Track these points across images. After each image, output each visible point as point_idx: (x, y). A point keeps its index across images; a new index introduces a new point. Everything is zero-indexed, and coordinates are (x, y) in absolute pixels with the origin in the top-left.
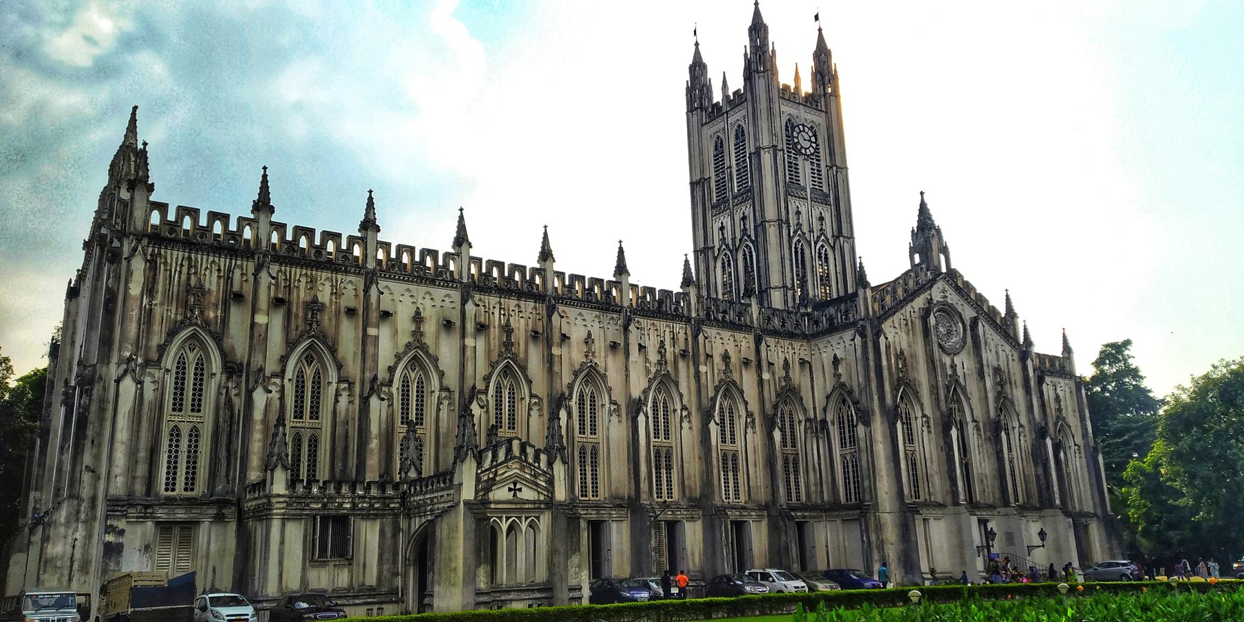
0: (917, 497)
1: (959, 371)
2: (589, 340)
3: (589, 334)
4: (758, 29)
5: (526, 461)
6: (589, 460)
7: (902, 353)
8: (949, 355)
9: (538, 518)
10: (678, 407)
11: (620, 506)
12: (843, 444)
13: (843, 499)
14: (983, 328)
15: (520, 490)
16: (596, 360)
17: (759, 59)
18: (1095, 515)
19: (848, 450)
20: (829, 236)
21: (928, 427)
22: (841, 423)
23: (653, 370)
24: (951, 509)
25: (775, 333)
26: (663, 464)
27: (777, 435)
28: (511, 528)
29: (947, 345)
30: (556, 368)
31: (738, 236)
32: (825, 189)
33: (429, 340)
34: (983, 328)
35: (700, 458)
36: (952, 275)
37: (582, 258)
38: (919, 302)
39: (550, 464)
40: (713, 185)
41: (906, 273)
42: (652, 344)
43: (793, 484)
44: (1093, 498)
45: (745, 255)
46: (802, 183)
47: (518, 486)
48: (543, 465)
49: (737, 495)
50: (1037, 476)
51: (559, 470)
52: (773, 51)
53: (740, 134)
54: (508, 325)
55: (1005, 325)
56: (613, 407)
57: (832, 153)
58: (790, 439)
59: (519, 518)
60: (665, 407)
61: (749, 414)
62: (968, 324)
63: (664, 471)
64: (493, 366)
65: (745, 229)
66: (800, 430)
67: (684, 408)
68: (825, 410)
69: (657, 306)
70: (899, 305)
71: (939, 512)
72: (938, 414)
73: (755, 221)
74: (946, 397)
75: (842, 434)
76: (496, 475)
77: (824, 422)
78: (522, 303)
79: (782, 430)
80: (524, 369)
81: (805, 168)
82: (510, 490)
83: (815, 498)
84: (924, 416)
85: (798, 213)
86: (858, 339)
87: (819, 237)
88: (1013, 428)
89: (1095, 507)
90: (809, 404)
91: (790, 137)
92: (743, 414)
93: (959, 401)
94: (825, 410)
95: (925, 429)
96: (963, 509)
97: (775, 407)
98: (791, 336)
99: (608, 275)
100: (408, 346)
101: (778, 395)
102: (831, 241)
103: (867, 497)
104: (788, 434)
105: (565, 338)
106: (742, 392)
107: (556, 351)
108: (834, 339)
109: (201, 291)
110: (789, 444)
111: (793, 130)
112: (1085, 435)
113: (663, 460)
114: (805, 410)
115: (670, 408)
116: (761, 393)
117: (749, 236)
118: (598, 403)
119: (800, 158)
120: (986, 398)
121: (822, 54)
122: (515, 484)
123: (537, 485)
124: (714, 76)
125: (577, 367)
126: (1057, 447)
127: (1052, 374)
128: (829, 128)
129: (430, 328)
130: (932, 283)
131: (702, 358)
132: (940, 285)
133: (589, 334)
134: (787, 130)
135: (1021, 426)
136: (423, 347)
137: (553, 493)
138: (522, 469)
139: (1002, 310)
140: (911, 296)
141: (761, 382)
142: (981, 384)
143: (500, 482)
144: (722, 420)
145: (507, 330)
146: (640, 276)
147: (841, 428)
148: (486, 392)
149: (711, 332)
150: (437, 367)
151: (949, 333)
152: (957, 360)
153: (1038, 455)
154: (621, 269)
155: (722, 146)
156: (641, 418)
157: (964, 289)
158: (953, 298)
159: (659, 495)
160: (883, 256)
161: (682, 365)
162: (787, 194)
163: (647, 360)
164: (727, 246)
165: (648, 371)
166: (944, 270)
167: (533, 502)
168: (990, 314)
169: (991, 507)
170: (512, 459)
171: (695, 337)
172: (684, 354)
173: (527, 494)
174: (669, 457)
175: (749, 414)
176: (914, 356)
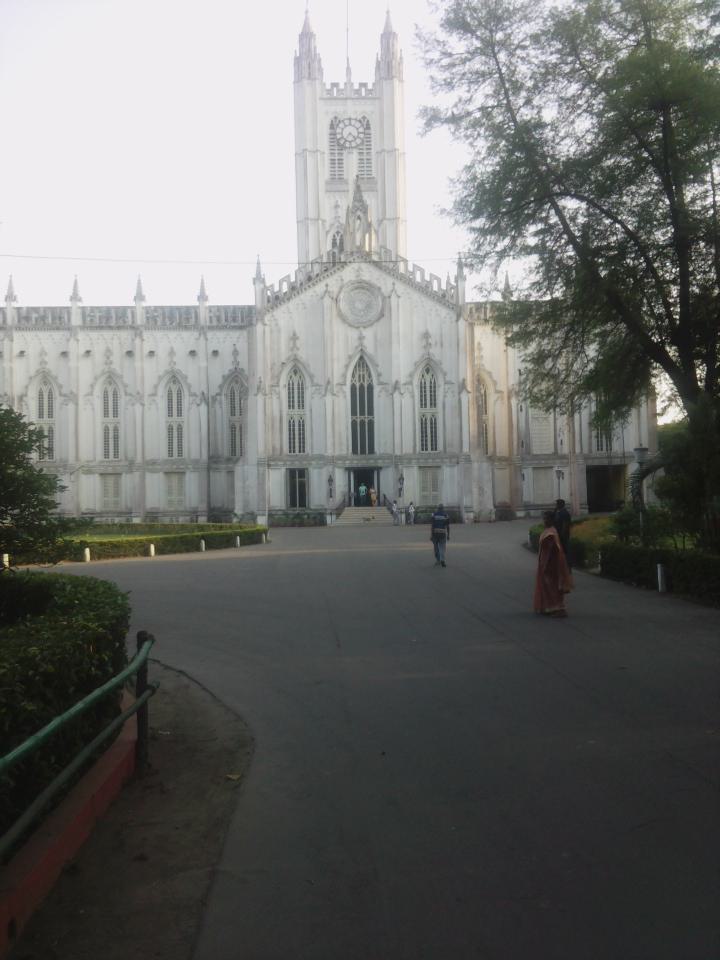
4: (306, 36)
8: (358, 328)
42: (98, 352)
46: (345, 177)
85: (337, 206)
91: (333, 135)
119: (345, 152)
132: (355, 266)
144: (170, 401)
158: (369, 274)
166: (367, 249)
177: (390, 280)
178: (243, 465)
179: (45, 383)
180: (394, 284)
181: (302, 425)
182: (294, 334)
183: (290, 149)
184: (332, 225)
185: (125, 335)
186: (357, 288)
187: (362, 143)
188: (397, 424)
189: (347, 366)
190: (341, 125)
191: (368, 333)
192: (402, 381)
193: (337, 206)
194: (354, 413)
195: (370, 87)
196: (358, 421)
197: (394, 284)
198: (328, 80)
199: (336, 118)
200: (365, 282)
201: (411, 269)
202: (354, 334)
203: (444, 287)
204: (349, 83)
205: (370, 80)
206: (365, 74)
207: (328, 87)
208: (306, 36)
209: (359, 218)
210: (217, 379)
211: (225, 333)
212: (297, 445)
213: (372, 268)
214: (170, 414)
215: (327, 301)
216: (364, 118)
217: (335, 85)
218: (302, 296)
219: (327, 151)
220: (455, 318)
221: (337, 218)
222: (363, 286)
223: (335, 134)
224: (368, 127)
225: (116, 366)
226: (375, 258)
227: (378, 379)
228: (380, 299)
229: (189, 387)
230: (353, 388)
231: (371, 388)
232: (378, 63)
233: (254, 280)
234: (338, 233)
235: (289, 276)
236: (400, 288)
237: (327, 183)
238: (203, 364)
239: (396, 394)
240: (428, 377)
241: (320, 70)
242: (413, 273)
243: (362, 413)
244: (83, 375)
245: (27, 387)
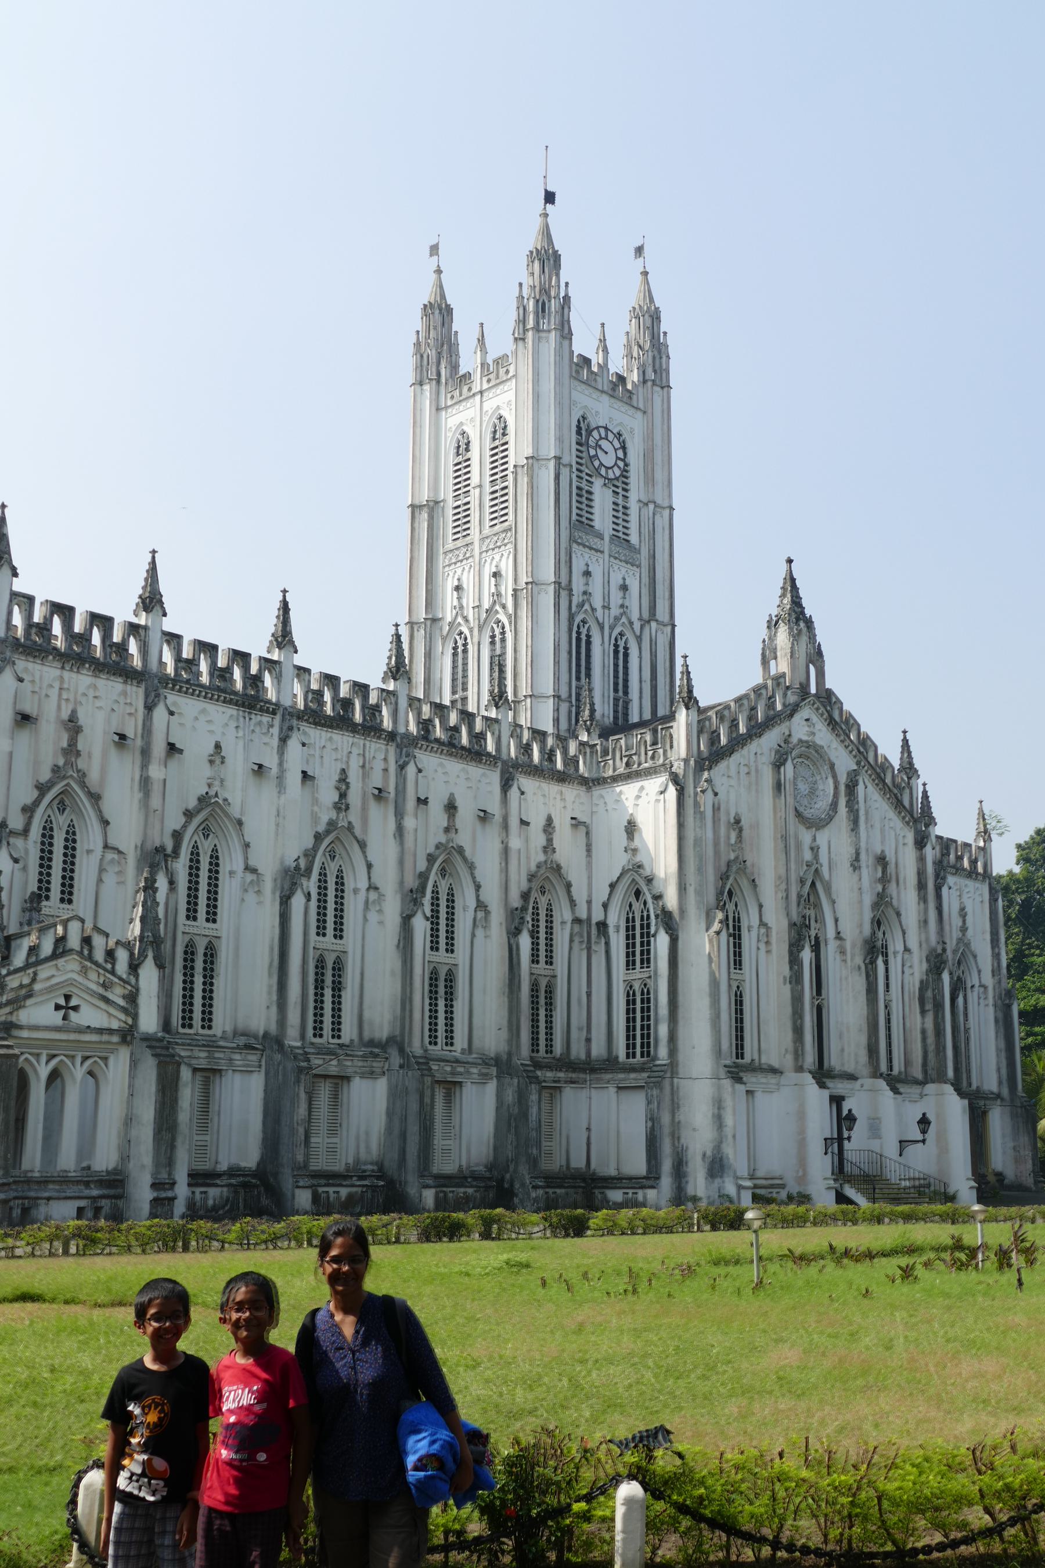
0: (740, 1055)
1: (824, 858)
3: (218, 746)
5: (90, 958)
6: (199, 965)
7: (738, 821)
9: (105, 1059)
10: (363, 884)
11: (248, 1047)
12: (630, 964)
13: (621, 1052)
14: (867, 791)
15: (75, 1008)
16: (223, 794)
17: (546, 308)
18: (999, 1096)
19: (638, 974)
20: (635, 616)
21: (767, 943)
22: (630, 928)
23: (326, 816)
24: (791, 1076)
25: (536, 772)
26: (329, 979)
27: (525, 941)
28: (54, 1076)
29: (808, 813)
30: (155, 802)
31: (486, 605)
32: (634, 539)
34: (867, 791)
35: (393, 973)
36: (827, 699)
37: (217, 613)
38: (771, 739)
39: (134, 967)
40: (450, 512)
41: (757, 690)
43: (542, 1025)
44: (999, 1070)
45: (493, 637)
46: (597, 524)
47: (73, 1002)
48: (122, 966)
49: (450, 1040)
50: (923, 1032)
51: (149, 976)
52: (567, 298)
53: (500, 430)
54: (73, 719)
55: (899, 786)
56: (250, 877)
57: (650, 480)
58: (544, 951)
59: (72, 1058)
60: (340, 882)
61: (481, 906)
62: (843, 779)
63: (328, 993)
65: (499, 595)
66: (562, 937)
67: (372, 887)
68: (605, 906)
69: (341, 711)
70: (738, 742)
71: (772, 1079)
72: (785, 923)
73: (516, 580)
74: (799, 896)
75: (630, 946)
76: (34, 980)
77: (602, 926)
79: (534, 934)
81: (602, 498)
82: (58, 1007)
83: (578, 1051)
84: (762, 924)
85: (587, 574)
86: (672, 791)
87: (617, 619)
88: (895, 953)
89: (1000, 1083)
90: (579, 893)
92: (472, 903)
93: (818, 906)
94: (605, 906)
95: (762, 946)
96: (808, 1078)
97: (525, 896)
98: (562, 778)
99: (258, 645)
101: (531, 877)
102: (637, 626)
103: (663, 1052)
104: (542, 941)
105: (172, 749)
106: (471, 867)
107: (156, 772)
108: (628, 791)
110: (542, 959)
111: (589, 432)
112: (995, 972)
113: (329, 973)
114: (573, 903)
115: (349, 885)
116: (505, 870)
117: (504, 607)
118: (224, 868)
120: (861, 902)
122: (68, 998)
123: (107, 1000)
124: (464, 327)
126: (958, 986)
127: (958, 870)
128: (649, 437)
130: (792, 711)
131: (411, 804)
132: (805, 712)
133: (218, 746)
134: (579, 432)
135: (907, 949)
137: (135, 1017)
138: (84, 971)
139: (896, 764)
140: (757, 730)
141: (506, 851)
142: (855, 877)
143: (43, 992)
144: (435, 912)
145: (73, 726)
146: (315, 653)
147: (630, 937)
148: (26, 832)
149: (427, 760)
151: (812, 792)
152: (823, 838)
153: (928, 997)
154: (284, 638)
155: (467, 450)
156: (298, 902)
157: (842, 724)
158: (823, 736)
159: (318, 1032)
160: (721, 657)
161: (375, 810)
162: (572, 540)
164: (466, 620)
165: (315, 819)
166: (813, 690)
167: (100, 1031)
168: (879, 770)
169: (852, 1077)
170: (66, 952)
171: (402, 767)
172: (380, 794)
173: (90, 1015)
174: (339, 967)
175: (481, 905)
176: (756, 826)
178: (672, 1078)
184: (581, 605)
185: (378, 750)
186: (800, 756)
187: (617, 479)
190: (595, 434)
202: (806, 836)
211: (537, 784)
218: (745, 751)
225: (354, 816)
228: (830, 781)
244: (274, 827)
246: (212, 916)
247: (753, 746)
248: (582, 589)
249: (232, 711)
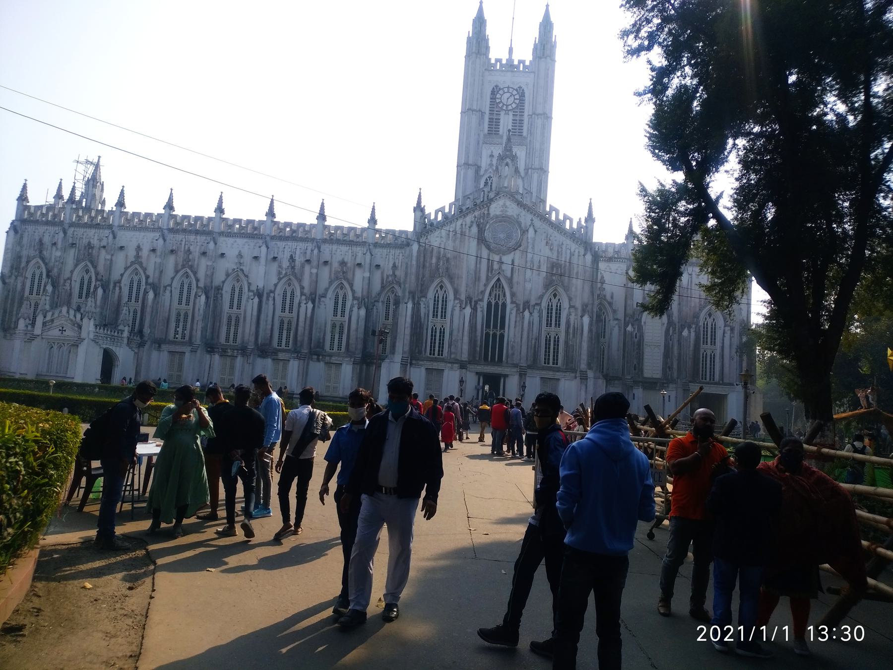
2: (240, 256)
4: (480, 22)
6: (233, 323)
23: (284, 272)
33: (144, 260)
46: (501, 133)
49: (339, 348)
63: (285, 332)
64: (177, 272)
78: (198, 237)
80: (195, 273)
85: (492, 156)
100: (132, 263)
109: (41, 242)
121: (546, 26)
125: (230, 271)
129: (145, 253)
132: (501, 202)
135: (571, 307)
136: (141, 264)
144: (336, 303)
150: (145, 273)
158: (513, 210)
163: (280, 267)
165: (280, 273)
177: (529, 216)
179: (238, 281)
180: (532, 220)
181: (442, 333)
182: (445, 256)
183: (459, 109)
184: (486, 171)
186: (500, 222)
188: (516, 332)
189: (486, 285)
190: (501, 92)
191: (507, 259)
192: (533, 302)
193: (492, 156)
194: (488, 326)
195: (527, 63)
196: (491, 333)
197: (532, 220)
198: (493, 55)
199: (497, 86)
200: (507, 217)
201: (548, 209)
202: (496, 258)
203: (575, 226)
204: (510, 60)
205: (528, 57)
206: (524, 53)
207: (493, 61)
208: (480, 22)
209: (507, 164)
210: (377, 286)
212: (437, 349)
213: (514, 206)
214: (335, 315)
215: (475, 230)
216: (520, 87)
217: (498, 60)
218: (453, 225)
219: (487, 112)
220: (582, 252)
221: (491, 165)
222: (504, 219)
223: (495, 99)
224: (522, 95)
226: (519, 197)
227: (512, 298)
229: (353, 292)
230: (489, 304)
231: (504, 305)
232: (535, 45)
233: (415, 210)
234: (490, 177)
235: (444, 208)
236: (537, 223)
237: (485, 135)
238: (367, 275)
239: (527, 313)
240: (555, 301)
241: (487, 48)
242: (550, 213)
243: (495, 327)
245: (224, 282)
246: (239, 307)
247: (459, 222)
248: (489, 162)
249: (245, 240)
